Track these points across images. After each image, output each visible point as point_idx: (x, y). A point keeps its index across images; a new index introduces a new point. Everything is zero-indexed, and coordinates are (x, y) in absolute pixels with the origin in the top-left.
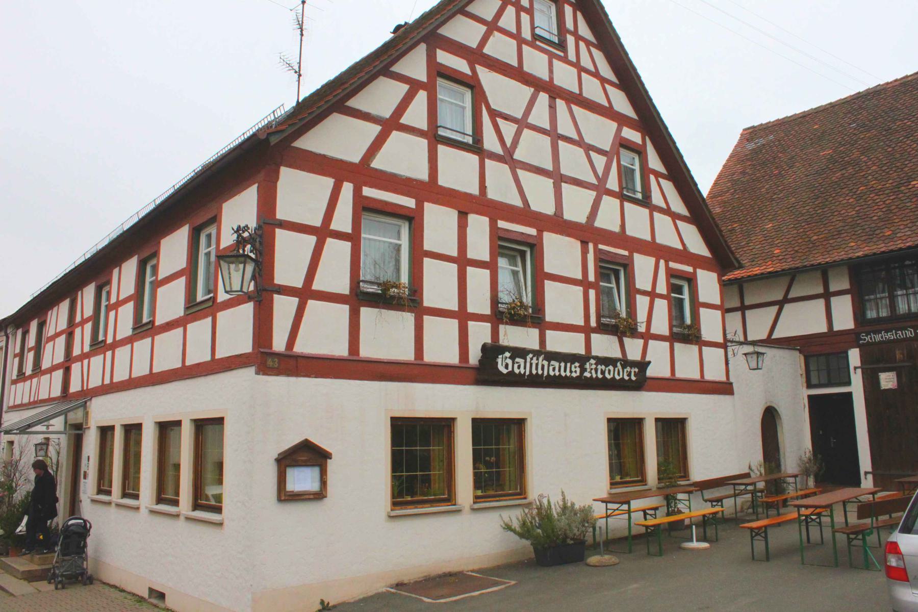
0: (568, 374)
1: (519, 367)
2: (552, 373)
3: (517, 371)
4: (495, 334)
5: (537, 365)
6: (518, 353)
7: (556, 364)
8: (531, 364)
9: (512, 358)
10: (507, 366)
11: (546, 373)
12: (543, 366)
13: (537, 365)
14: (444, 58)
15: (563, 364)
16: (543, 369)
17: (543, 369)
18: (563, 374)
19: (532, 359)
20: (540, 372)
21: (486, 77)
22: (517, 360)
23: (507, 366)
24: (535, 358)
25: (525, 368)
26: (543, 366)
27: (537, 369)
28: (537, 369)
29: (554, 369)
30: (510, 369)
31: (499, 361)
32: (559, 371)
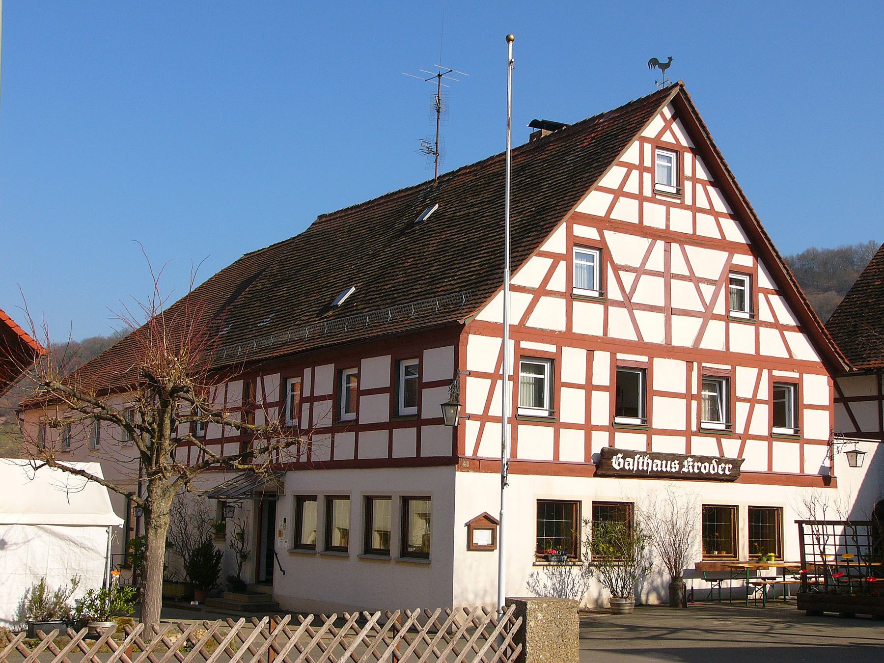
0: (669, 469)
1: (629, 465)
2: (655, 469)
3: (627, 467)
4: (612, 439)
5: (643, 462)
6: (627, 454)
7: (659, 462)
8: (638, 462)
9: (624, 458)
10: (619, 465)
11: (650, 469)
12: (648, 463)
13: (643, 462)
14: (581, 231)
15: (664, 462)
16: (648, 466)
17: (648, 466)
18: (664, 470)
19: (639, 459)
20: (645, 468)
21: (613, 239)
22: (627, 459)
23: (619, 465)
24: (641, 458)
25: (633, 465)
26: (648, 463)
27: (643, 466)
28: (643, 466)
29: (657, 466)
30: (622, 466)
31: (614, 460)
32: (661, 467)
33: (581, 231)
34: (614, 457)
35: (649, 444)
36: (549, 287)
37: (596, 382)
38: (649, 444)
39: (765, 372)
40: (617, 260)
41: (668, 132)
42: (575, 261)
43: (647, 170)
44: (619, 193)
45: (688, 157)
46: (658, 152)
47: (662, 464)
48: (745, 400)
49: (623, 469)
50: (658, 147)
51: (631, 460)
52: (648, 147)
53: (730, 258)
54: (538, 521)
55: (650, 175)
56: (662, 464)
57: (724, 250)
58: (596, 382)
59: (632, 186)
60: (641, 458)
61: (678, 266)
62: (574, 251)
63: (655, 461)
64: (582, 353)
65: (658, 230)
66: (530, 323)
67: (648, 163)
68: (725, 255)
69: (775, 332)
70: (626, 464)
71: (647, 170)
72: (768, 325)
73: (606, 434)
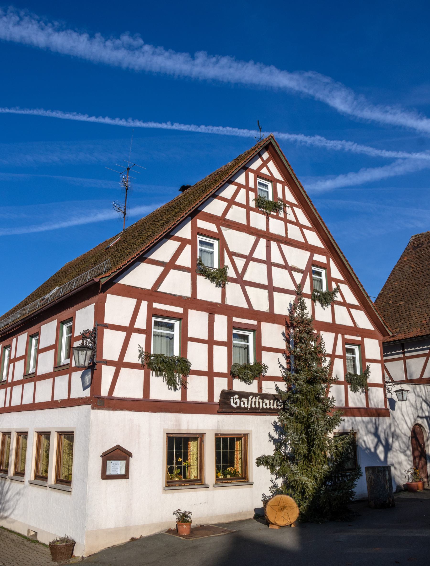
0: (275, 407)
1: (244, 404)
2: (265, 407)
3: (242, 406)
4: (230, 384)
5: (255, 402)
6: (243, 395)
7: (268, 401)
8: (252, 402)
9: (240, 398)
10: (236, 403)
11: (261, 407)
12: (259, 403)
13: (255, 402)
14: (202, 224)
15: (272, 401)
16: (259, 404)
17: (259, 404)
18: (272, 407)
19: (252, 399)
20: (257, 406)
21: (228, 233)
22: (243, 399)
23: (236, 403)
24: (254, 398)
25: (248, 404)
26: (259, 403)
27: (255, 404)
28: (255, 404)
29: (266, 405)
30: (238, 405)
31: (232, 400)
32: (270, 405)
33: (202, 224)
34: (232, 398)
35: (260, 387)
36: (178, 263)
37: (216, 338)
38: (260, 387)
39: (340, 336)
40: (231, 249)
41: (265, 168)
42: (199, 247)
43: (252, 190)
44: (231, 202)
45: (279, 186)
46: (259, 180)
47: (270, 403)
48: (329, 355)
49: (240, 407)
50: (259, 177)
51: (245, 400)
52: (251, 176)
53: (311, 256)
54: (168, 452)
55: (254, 194)
56: (270, 403)
57: (307, 250)
58: (216, 338)
59: (241, 198)
60: (254, 398)
61: (276, 258)
62: (198, 239)
63: (265, 400)
64: (205, 316)
65: (261, 231)
66: (162, 289)
67: (252, 184)
68: (308, 254)
69: (344, 309)
70: (242, 403)
71: (252, 190)
72: (339, 303)
73: (225, 380)
